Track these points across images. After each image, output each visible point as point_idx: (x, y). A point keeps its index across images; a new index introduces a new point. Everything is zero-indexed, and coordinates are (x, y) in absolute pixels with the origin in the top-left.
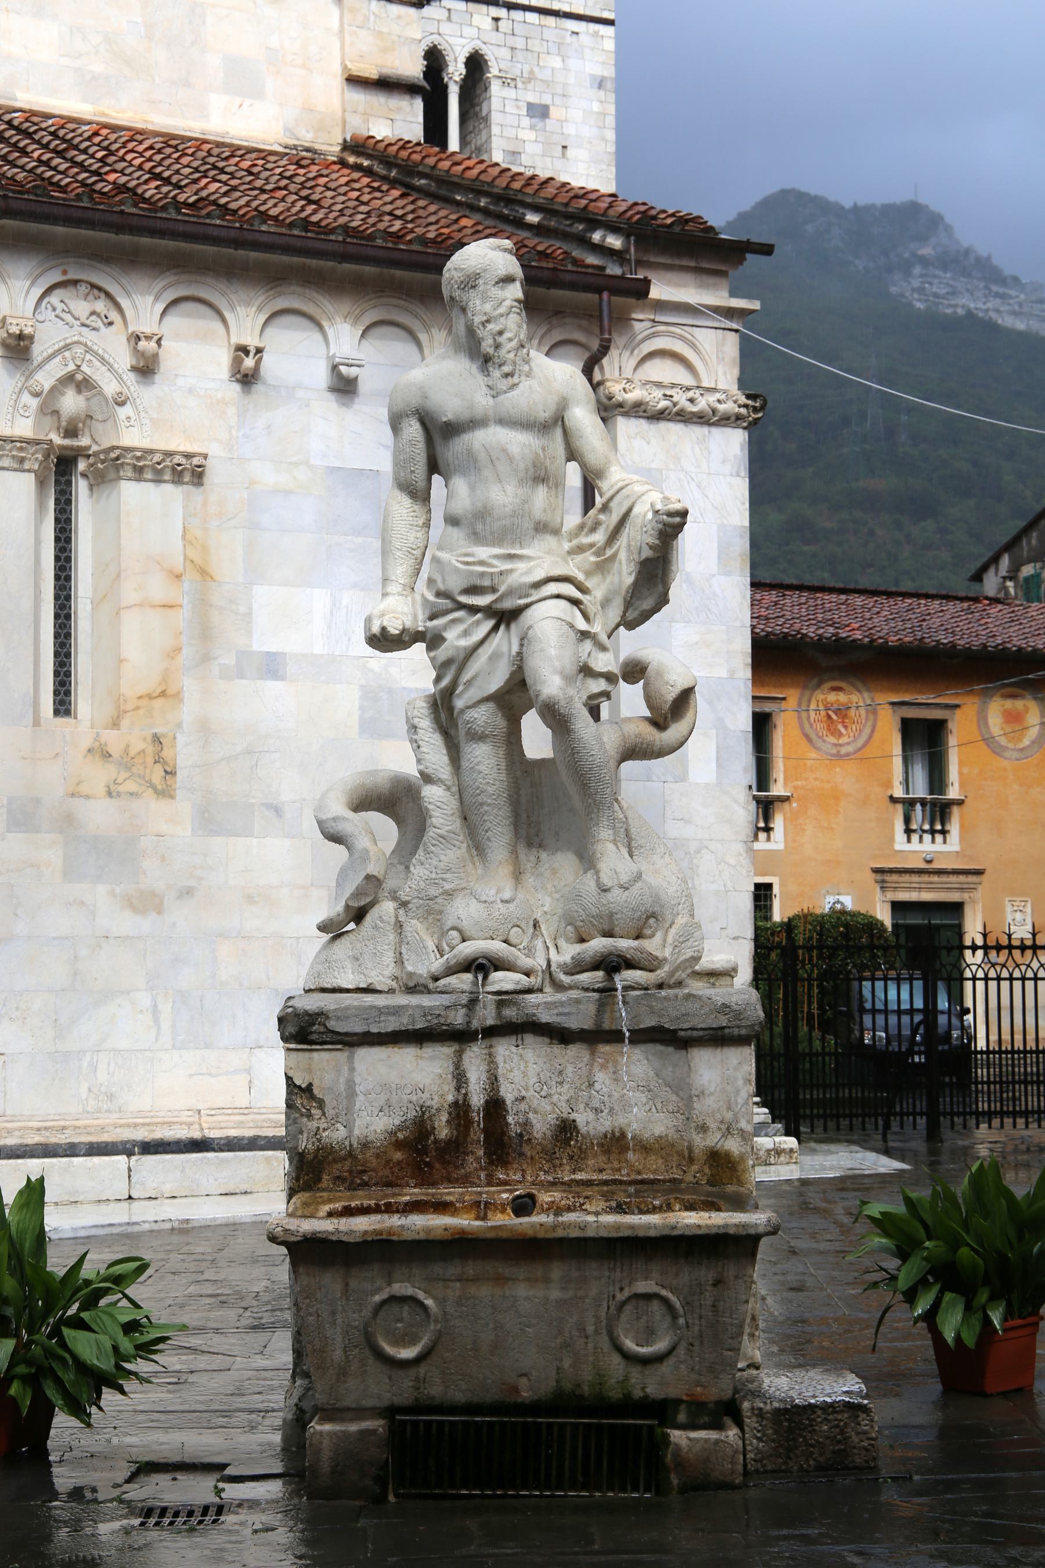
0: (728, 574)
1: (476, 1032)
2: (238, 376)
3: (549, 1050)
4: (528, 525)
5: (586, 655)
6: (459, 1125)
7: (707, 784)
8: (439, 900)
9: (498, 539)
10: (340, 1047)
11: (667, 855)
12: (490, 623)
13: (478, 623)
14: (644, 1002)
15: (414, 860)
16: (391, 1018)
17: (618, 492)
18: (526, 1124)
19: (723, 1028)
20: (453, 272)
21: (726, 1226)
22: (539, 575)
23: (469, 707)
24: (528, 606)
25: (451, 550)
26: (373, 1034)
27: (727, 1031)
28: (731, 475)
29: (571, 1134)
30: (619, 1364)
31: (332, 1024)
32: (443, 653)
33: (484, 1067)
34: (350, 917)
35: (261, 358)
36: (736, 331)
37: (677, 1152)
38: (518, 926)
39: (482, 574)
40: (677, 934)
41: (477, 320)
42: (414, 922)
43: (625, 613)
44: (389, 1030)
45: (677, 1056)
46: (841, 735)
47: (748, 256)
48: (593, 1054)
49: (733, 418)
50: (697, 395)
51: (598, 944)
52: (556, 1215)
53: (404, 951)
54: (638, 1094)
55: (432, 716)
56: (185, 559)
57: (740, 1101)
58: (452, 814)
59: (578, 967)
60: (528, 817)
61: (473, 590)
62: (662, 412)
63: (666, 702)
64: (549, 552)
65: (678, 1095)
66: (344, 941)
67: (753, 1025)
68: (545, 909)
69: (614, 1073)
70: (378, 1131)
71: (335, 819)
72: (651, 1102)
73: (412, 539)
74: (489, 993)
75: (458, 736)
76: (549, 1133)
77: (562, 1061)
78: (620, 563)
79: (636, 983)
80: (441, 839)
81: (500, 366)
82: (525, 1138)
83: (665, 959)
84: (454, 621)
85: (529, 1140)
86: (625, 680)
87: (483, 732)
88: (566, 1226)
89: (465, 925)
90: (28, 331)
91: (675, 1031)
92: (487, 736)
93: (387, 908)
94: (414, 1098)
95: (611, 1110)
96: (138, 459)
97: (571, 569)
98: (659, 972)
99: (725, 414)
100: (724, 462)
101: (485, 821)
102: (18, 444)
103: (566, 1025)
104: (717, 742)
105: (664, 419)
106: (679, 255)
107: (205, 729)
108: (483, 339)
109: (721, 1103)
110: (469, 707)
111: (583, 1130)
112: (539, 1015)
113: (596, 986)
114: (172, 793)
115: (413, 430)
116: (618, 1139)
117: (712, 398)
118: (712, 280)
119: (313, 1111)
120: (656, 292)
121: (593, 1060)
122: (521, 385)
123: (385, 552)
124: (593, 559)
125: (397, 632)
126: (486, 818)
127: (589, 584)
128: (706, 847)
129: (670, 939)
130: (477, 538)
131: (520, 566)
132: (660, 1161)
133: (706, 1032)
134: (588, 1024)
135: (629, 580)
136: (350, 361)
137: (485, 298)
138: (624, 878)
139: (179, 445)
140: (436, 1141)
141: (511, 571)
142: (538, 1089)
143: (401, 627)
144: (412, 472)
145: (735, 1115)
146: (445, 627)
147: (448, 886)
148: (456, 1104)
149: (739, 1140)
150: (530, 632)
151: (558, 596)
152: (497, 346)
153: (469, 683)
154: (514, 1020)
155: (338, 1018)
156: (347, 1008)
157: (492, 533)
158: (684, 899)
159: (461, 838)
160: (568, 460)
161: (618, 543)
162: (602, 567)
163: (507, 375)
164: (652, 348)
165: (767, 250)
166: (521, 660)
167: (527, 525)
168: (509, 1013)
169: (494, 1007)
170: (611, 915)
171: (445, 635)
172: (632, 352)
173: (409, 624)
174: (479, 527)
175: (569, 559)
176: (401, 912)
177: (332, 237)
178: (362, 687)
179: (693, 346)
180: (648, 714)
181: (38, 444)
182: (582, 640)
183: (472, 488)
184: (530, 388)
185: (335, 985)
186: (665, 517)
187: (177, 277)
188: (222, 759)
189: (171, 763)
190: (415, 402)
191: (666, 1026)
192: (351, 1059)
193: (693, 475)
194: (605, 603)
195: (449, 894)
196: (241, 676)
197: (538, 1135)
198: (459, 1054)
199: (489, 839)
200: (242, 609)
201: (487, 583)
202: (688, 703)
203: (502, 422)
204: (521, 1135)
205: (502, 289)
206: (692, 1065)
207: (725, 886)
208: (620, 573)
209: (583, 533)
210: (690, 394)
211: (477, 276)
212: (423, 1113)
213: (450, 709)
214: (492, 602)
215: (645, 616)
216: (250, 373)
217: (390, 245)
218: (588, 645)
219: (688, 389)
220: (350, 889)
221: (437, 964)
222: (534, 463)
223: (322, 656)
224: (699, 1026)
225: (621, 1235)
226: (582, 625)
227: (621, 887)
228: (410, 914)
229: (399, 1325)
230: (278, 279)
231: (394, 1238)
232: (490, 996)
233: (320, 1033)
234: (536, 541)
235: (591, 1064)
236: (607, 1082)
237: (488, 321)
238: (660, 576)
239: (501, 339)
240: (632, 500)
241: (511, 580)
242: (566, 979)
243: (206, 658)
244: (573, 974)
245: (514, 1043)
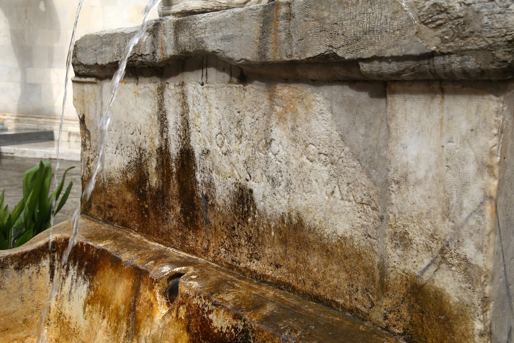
3: (229, 90)
6: (163, 174)
10: (93, 80)
18: (210, 185)
19: (432, 55)
27: (439, 61)
29: (249, 208)
33: (179, 110)
37: (365, 269)
45: (373, 109)
48: (271, 98)
54: (318, 166)
57: (468, 205)
65: (369, 177)
67: (490, 49)
69: (293, 129)
72: (334, 182)
74: (175, 14)
76: (229, 202)
77: (240, 107)
82: (210, 203)
85: (213, 205)
91: (355, 63)
95: (289, 183)
109: (434, 202)
111: (260, 206)
116: (295, 228)
121: (272, 108)
132: (343, 275)
133: (403, 65)
140: (150, 189)
145: (457, 229)
148: (160, 149)
149: (460, 277)
191: (340, 53)
197: (220, 202)
198: (161, 90)
204: (206, 197)
206: (392, 125)
224: (388, 53)
235: (268, 115)
236: (285, 142)
245: (200, 80)
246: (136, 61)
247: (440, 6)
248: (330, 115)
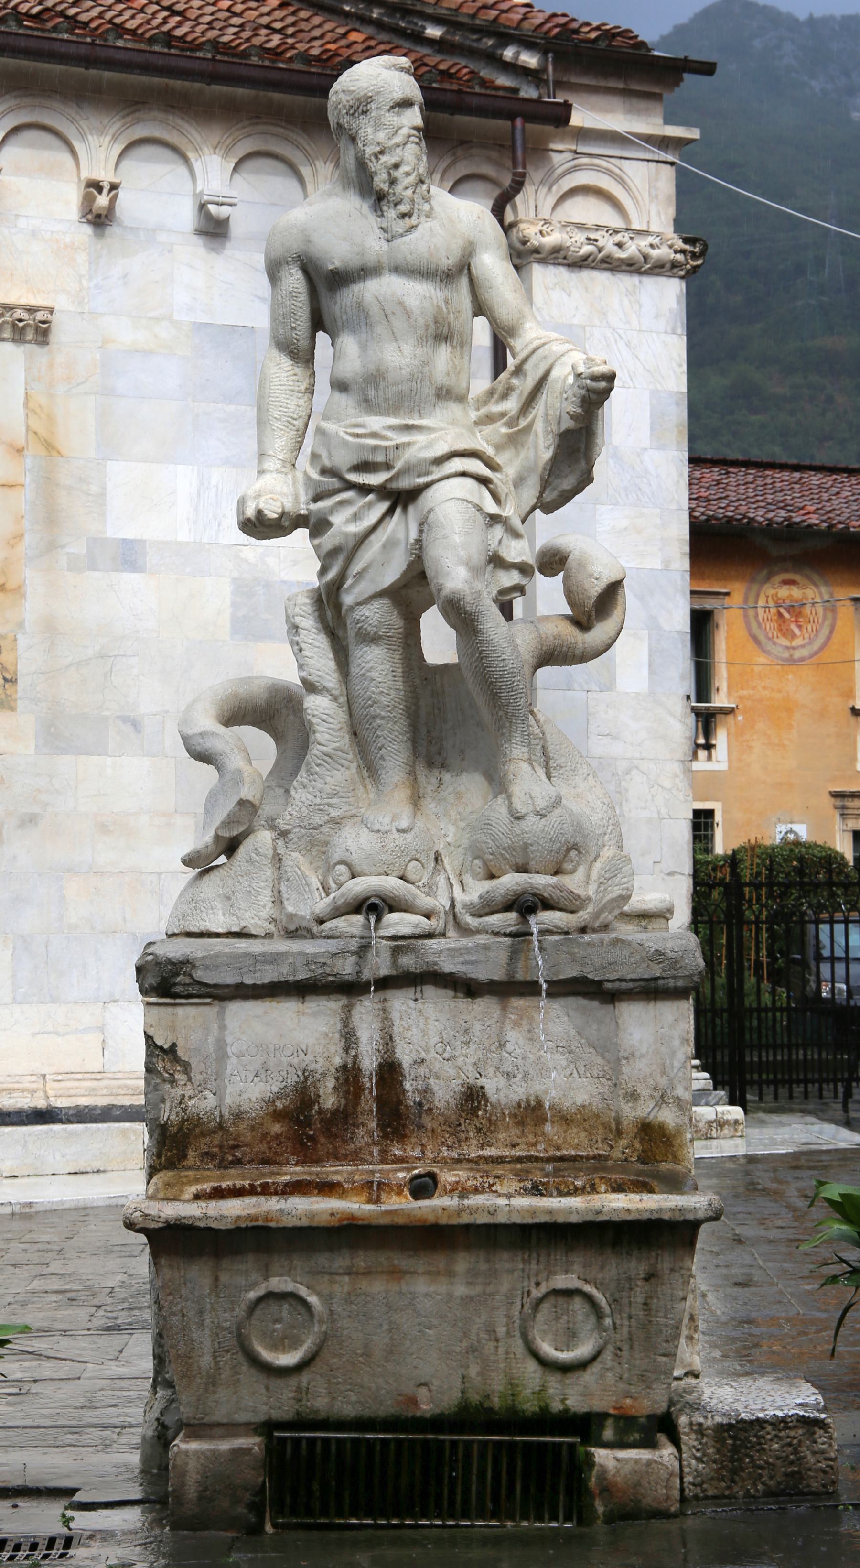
0: (662, 447)
1: (367, 984)
3: (453, 1005)
4: (428, 391)
5: (496, 543)
6: (348, 1092)
7: (638, 694)
8: (325, 829)
9: (394, 407)
10: (208, 1000)
11: (591, 777)
12: (384, 506)
13: (370, 505)
14: (565, 949)
15: (295, 783)
16: (269, 968)
17: (534, 352)
18: (426, 1091)
19: (656, 979)
20: (341, 95)
22: (441, 449)
23: (359, 604)
24: (428, 485)
25: (339, 420)
26: (247, 986)
27: (661, 982)
28: (666, 332)
29: (479, 1103)
31: (199, 975)
32: (328, 540)
33: (377, 1025)
34: (220, 849)
35: (116, 197)
36: (672, 164)
37: (603, 1124)
38: (416, 860)
39: (375, 449)
40: (602, 869)
41: (369, 150)
42: (295, 855)
43: (541, 493)
44: (266, 981)
45: (603, 1012)
46: (794, 636)
47: (686, 76)
48: (504, 1008)
49: (668, 266)
50: (626, 239)
51: (510, 881)
52: (461, 1197)
53: (283, 888)
54: (557, 1056)
55: (317, 614)
56: (27, 431)
57: (677, 1064)
58: (340, 729)
59: (487, 908)
60: (428, 732)
61: (364, 467)
62: (585, 258)
63: (589, 598)
64: (454, 423)
65: (603, 1058)
66: (214, 876)
67: (691, 976)
68: (449, 839)
69: (529, 1031)
70: (254, 1099)
71: (202, 735)
72: (572, 1066)
73: (292, 408)
74: (382, 938)
75: (346, 638)
76: (453, 1102)
77: (468, 1018)
78: (536, 435)
79: (555, 926)
80: (326, 758)
81: (396, 205)
82: (426, 1108)
83: (589, 899)
84: (342, 503)
85: (430, 1109)
87: (376, 633)
88: (473, 1210)
89: (355, 858)
91: (600, 983)
92: (380, 637)
93: (263, 838)
94: (295, 1061)
95: (526, 1074)
97: (480, 442)
98: (581, 913)
99: (658, 260)
100: (657, 316)
101: (378, 737)
103: (473, 976)
104: (650, 645)
105: (589, 267)
106: (606, 75)
108: (376, 173)
109: (654, 1067)
110: (359, 604)
111: (493, 1097)
112: (442, 964)
113: (508, 930)
114: (12, 704)
115: (294, 279)
116: (534, 1109)
117: (643, 243)
118: (642, 104)
119: (177, 1076)
120: (577, 119)
121: (505, 1016)
122: (419, 227)
123: (261, 423)
124: (504, 430)
125: (275, 516)
126: (379, 733)
127: (499, 460)
128: (637, 767)
129: (594, 875)
130: (369, 405)
131: (419, 438)
132: (583, 1134)
133: (637, 984)
134: (498, 974)
135: (547, 455)
136: (221, 200)
137: (378, 126)
138: (541, 804)
139: (20, 297)
140: (321, 1112)
141: (409, 444)
142: (440, 1050)
143: (280, 511)
144: (293, 328)
145: (671, 1081)
146: (332, 510)
147: (334, 813)
148: (344, 1067)
149: (675, 1109)
150: (431, 516)
151: (464, 474)
152: (393, 182)
153: (359, 576)
154: (412, 970)
155: (206, 968)
156: (217, 956)
157: (386, 400)
158: (610, 828)
159: (350, 757)
160: (476, 315)
161: (534, 412)
162: (514, 440)
163: (403, 216)
164: (573, 184)
165: (707, 69)
166: (421, 548)
167: (427, 390)
168: (407, 962)
169: (388, 954)
170: (526, 847)
171: (331, 519)
172: (550, 189)
173: (289, 506)
174: (372, 393)
175: (477, 430)
176: (280, 843)
177: (200, 54)
178: (235, 580)
179: (622, 182)
180: (569, 612)
182: (491, 526)
183: (363, 347)
184: (431, 230)
185: (202, 928)
186: (588, 381)
187: (18, 101)
188: (71, 665)
189: (11, 669)
190: (296, 246)
192: (221, 1015)
193: (621, 332)
194: (519, 482)
195: (337, 823)
196: (93, 567)
198: (348, 1010)
199: (382, 758)
200: (94, 489)
201: (380, 458)
202: (616, 599)
203: (398, 270)
204: (420, 1104)
206: (620, 1021)
207: (659, 812)
208: (536, 447)
209: (493, 400)
210: (618, 238)
211: (369, 99)
212: (306, 1078)
213: (337, 606)
214: (387, 481)
215: (566, 497)
216: (104, 213)
217: (267, 63)
218: (498, 531)
219: (616, 232)
220: (220, 816)
221: (322, 904)
222: (435, 318)
223: (187, 543)
224: (629, 977)
226: (491, 507)
227: (538, 813)
228: (290, 845)
230: (137, 103)
232: (384, 942)
233: (185, 985)
234: (437, 409)
235: (502, 1021)
236: (521, 1042)
237: (382, 152)
238: (582, 450)
239: (396, 174)
240: (550, 361)
242: (472, 922)
243: (52, 546)
244: (481, 916)
248: (566, 1018)
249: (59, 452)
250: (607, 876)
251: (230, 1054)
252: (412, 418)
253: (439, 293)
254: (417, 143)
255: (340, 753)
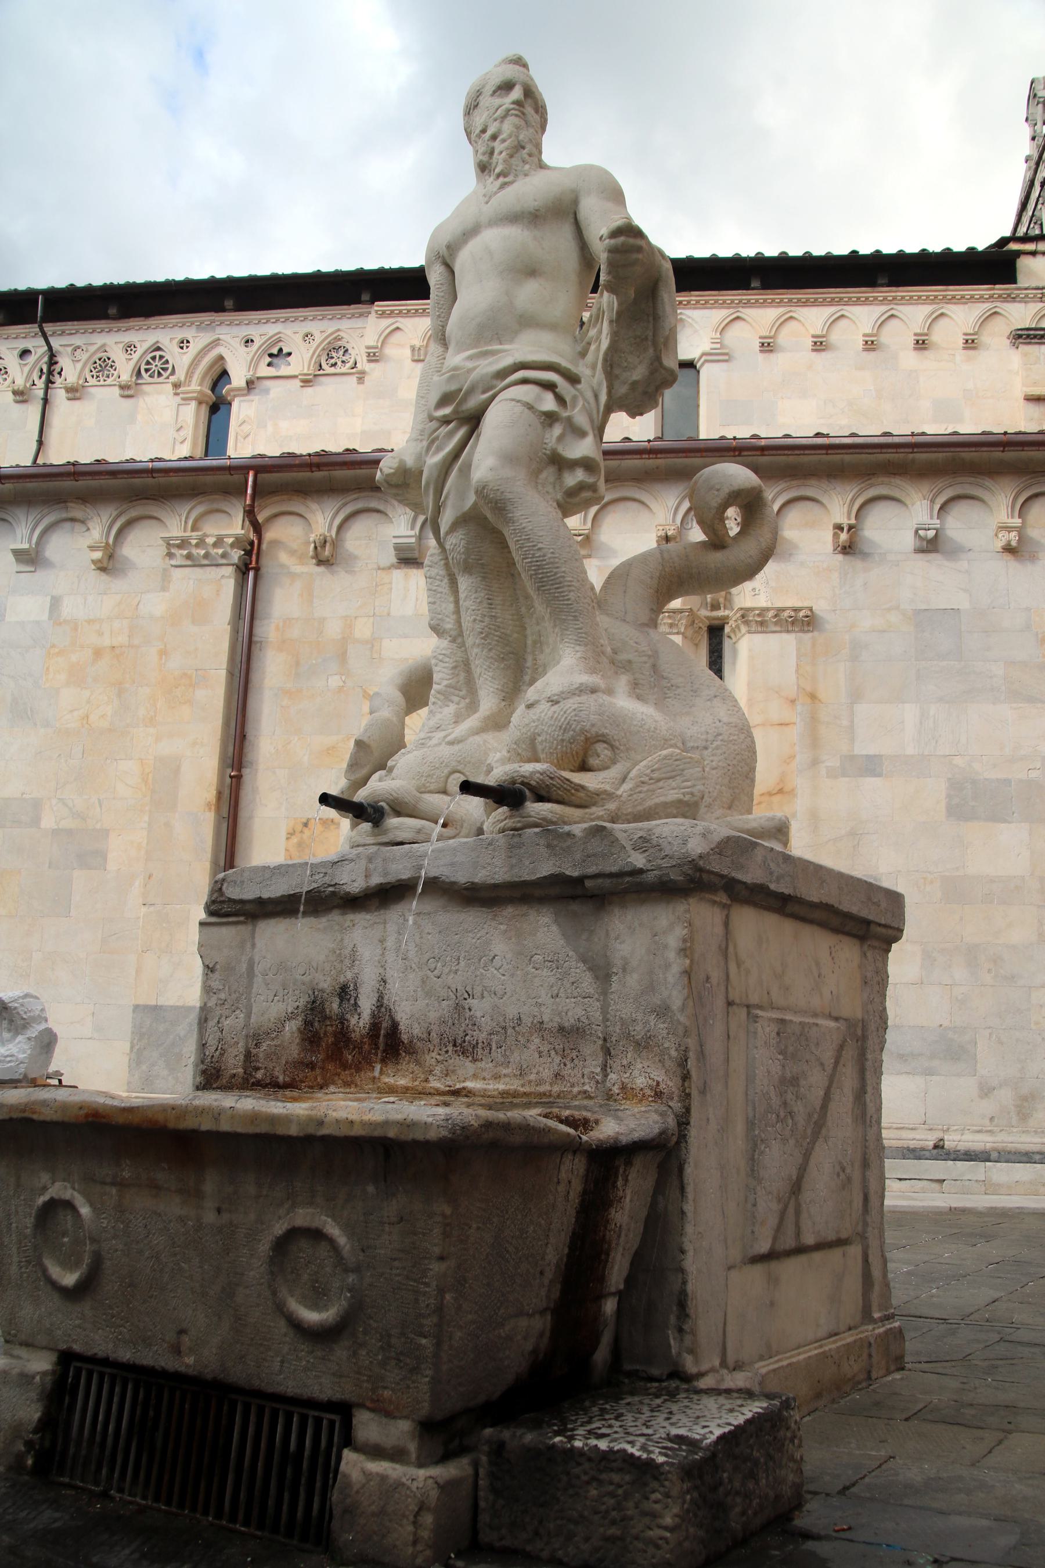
2: (839, 549)
5: (554, 440)
10: (242, 919)
13: (451, 434)
21: (386, 1123)
30: (285, 1335)
38: (459, 772)
40: (647, 767)
56: (798, 688)
58: (455, 668)
70: (272, 1019)
79: (544, 819)
80: (438, 696)
86: (592, 460)
90: (669, 533)
96: (759, 615)
98: (594, 809)
102: (667, 614)
107: (814, 816)
122: (515, 185)
125: (392, 471)
143: (396, 465)
151: (525, 381)
158: (719, 743)
159: (463, 693)
181: (681, 613)
186: (607, 241)
187: (788, 484)
191: (567, 873)
201: (453, 387)
205: (500, 96)
218: (557, 430)
225: (258, 1130)
229: (66, 1240)
231: (35, 1117)
241: (474, 376)
246: (324, 891)
247: (645, 838)
249: (820, 700)
250: (655, 775)
251: (256, 972)
252: (491, 345)
253: (526, 233)
254: (516, 115)
255: (452, 690)
